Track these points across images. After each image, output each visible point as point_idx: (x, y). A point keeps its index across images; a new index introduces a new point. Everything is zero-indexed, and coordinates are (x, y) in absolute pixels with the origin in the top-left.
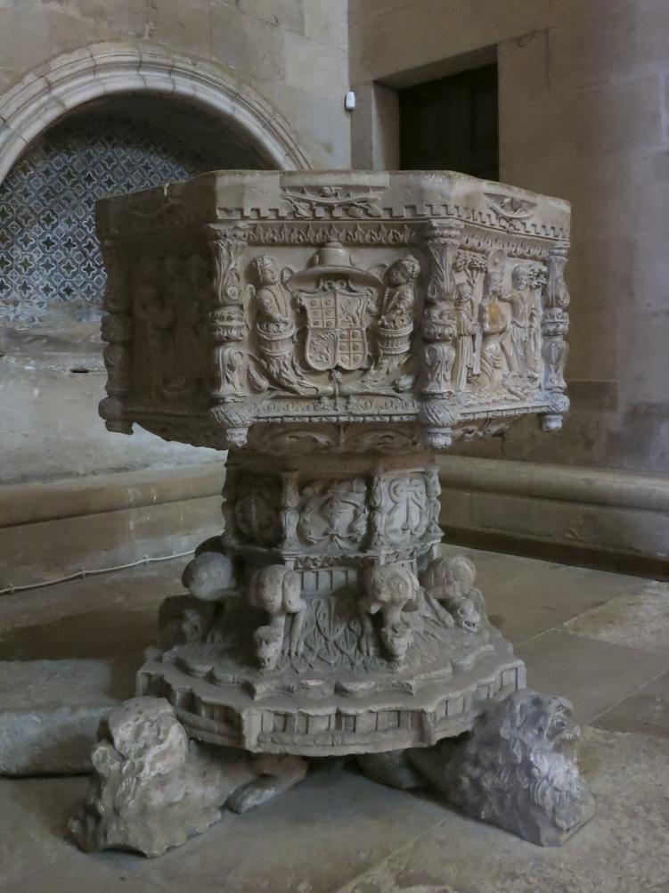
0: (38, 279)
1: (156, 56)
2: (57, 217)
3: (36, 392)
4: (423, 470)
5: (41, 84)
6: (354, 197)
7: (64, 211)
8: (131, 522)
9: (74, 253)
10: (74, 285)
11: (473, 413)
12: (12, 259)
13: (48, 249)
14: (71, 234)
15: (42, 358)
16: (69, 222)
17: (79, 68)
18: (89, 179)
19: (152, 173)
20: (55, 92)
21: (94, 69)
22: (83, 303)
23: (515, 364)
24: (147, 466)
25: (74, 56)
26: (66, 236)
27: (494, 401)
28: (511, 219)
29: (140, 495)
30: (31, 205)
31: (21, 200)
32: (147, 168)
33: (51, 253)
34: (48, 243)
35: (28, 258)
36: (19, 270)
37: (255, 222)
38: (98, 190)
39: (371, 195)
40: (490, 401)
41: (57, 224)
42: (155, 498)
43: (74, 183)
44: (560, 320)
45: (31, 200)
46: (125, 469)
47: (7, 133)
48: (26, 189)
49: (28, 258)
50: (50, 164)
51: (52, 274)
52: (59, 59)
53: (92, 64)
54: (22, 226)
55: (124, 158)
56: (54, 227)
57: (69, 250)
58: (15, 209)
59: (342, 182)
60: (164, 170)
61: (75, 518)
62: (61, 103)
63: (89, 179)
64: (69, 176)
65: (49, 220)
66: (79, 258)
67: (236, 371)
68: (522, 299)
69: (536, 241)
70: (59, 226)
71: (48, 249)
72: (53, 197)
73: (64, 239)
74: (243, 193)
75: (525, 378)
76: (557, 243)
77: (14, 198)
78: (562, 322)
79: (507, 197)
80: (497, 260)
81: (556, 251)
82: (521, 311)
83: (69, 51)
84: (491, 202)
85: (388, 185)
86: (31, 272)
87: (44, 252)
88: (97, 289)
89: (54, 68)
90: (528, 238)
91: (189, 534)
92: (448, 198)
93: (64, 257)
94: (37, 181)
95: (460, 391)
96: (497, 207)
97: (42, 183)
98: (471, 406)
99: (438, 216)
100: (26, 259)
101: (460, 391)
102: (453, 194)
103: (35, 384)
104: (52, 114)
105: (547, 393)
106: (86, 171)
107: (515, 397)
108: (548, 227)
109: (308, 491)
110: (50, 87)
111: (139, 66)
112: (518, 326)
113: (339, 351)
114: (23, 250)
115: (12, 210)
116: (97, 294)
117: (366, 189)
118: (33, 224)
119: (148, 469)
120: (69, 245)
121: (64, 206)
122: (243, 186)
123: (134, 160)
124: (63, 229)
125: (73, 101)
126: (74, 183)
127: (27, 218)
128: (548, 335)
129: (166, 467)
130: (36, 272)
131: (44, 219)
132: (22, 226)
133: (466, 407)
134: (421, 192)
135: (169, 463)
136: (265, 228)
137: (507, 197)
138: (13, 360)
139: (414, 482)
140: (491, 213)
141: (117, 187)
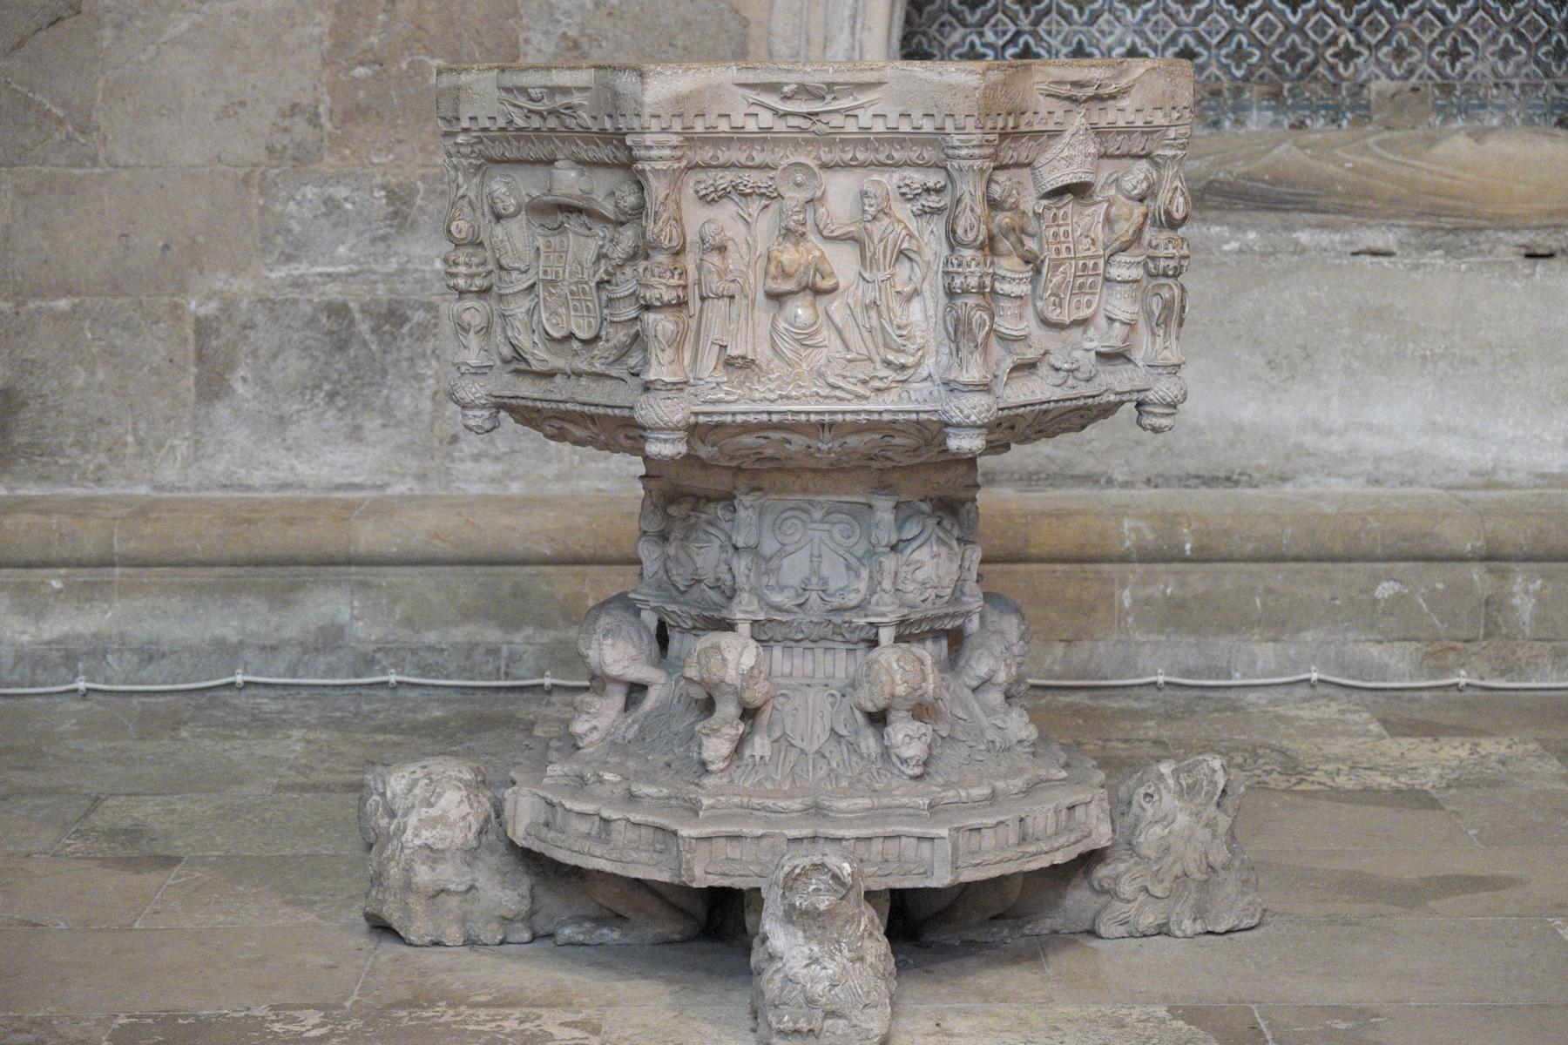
0: (1111, 33)
4: (862, 500)
6: (560, 100)
8: (1127, 592)
10: (1201, 40)
11: (734, 414)
22: (1226, 83)
23: (853, 337)
24: (1284, 479)
27: (788, 397)
28: (816, 114)
29: (1150, 536)
37: (479, 134)
39: (576, 99)
40: (773, 396)
42: (1188, 547)
44: (955, 269)
46: (1230, 481)
51: (1145, 19)
59: (543, 82)
61: (999, 567)
67: (472, 333)
68: (869, 234)
69: (894, 138)
74: (458, 98)
75: (879, 365)
76: (948, 138)
78: (958, 273)
79: (787, 84)
80: (799, 179)
81: (950, 152)
82: (868, 255)
84: (752, 95)
85: (593, 85)
86: (1094, 17)
88: (1261, 46)
90: (872, 137)
91: (1276, 640)
92: (642, 104)
95: (701, 379)
96: (774, 101)
98: (720, 401)
99: (632, 131)
101: (701, 379)
102: (648, 98)
105: (942, 389)
107: (838, 393)
108: (917, 115)
109: (673, 510)
112: (864, 279)
113: (572, 313)
116: (1262, 59)
117: (565, 91)
119: (1289, 488)
122: (458, 88)
128: (951, 293)
129: (1339, 486)
130: (1106, 16)
133: (713, 402)
134: (616, 95)
135: (1348, 477)
136: (493, 140)
137: (787, 84)
139: (833, 517)
140: (754, 109)
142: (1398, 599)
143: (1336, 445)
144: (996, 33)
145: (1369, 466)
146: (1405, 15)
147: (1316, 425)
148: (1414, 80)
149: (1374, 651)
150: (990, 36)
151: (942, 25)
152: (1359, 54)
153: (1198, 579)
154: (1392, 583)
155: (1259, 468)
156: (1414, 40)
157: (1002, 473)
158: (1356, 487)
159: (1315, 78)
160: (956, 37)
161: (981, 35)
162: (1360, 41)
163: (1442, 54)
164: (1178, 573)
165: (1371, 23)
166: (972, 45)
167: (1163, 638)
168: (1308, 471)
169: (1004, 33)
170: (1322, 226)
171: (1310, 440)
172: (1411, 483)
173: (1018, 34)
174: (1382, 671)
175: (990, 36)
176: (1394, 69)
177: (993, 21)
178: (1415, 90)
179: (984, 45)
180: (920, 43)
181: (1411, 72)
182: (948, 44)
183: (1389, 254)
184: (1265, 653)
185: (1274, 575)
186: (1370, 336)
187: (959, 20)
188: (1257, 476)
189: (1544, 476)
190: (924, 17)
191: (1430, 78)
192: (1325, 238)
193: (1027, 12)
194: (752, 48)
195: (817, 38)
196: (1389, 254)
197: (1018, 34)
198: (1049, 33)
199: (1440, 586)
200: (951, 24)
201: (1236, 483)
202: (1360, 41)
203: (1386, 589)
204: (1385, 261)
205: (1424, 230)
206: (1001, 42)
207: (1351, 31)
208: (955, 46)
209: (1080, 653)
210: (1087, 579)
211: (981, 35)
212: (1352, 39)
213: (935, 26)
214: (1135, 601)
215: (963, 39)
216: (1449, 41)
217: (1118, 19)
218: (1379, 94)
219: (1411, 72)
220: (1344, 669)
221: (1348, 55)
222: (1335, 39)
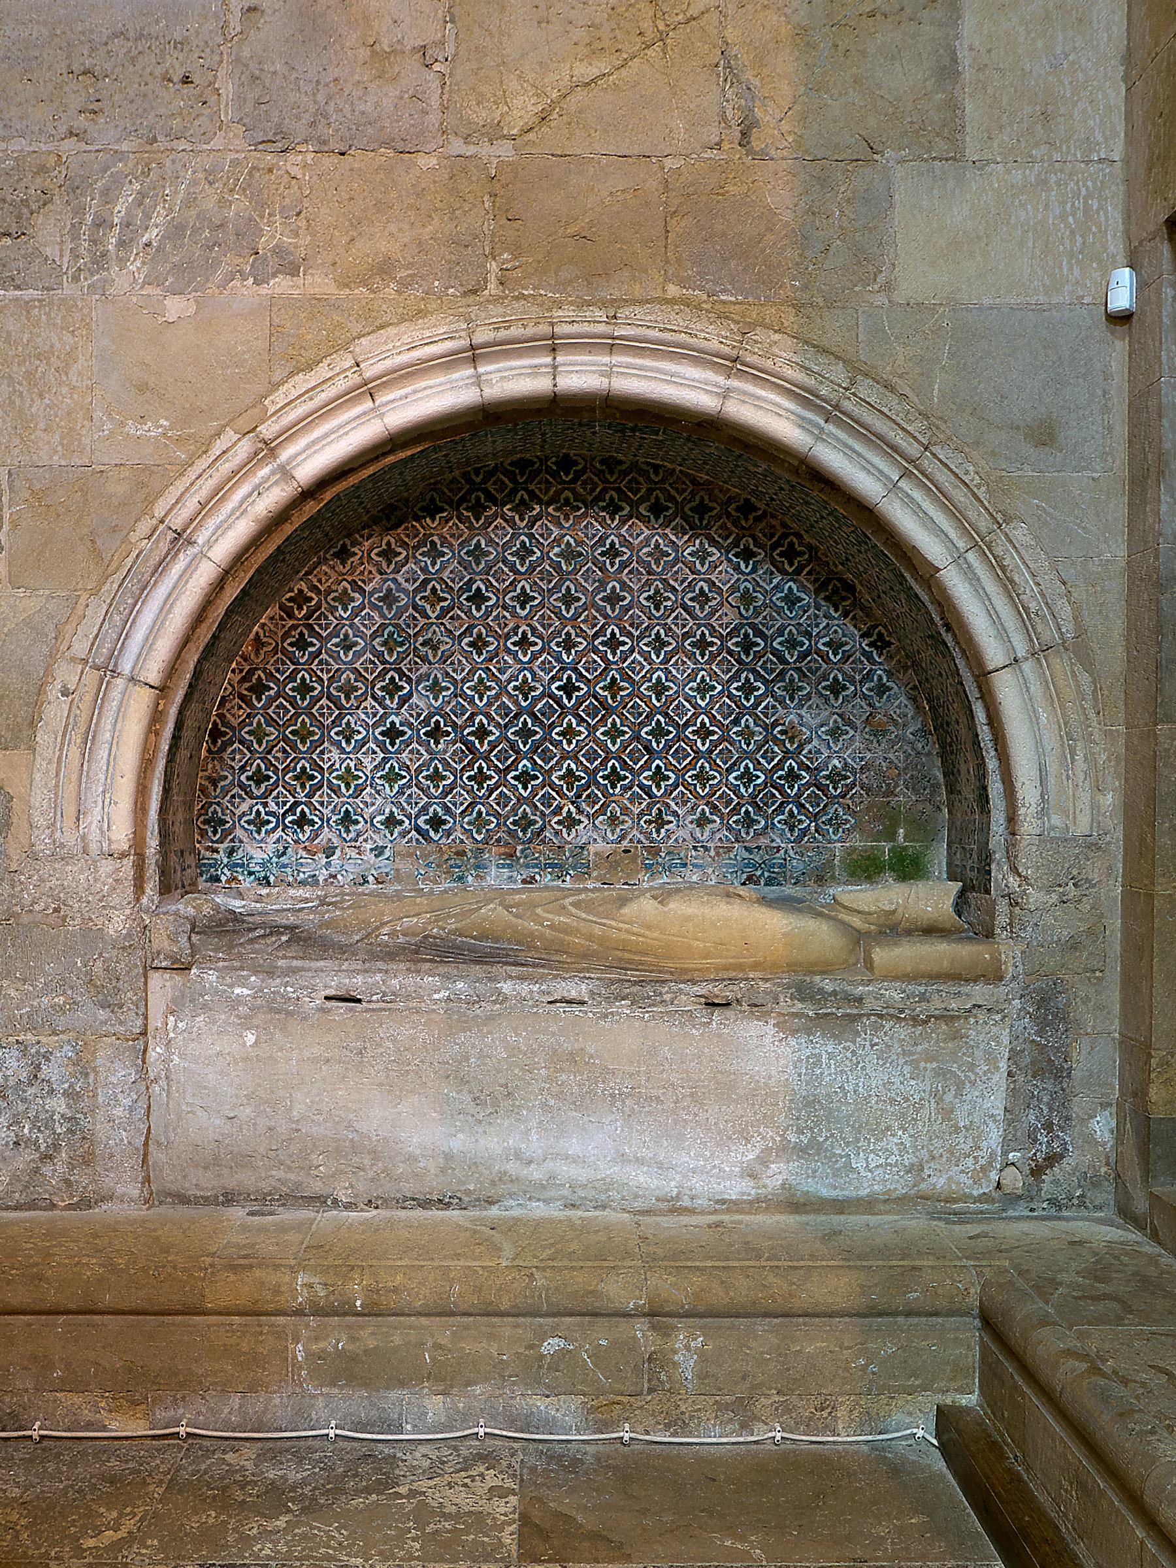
0: (373, 804)
1: (508, 325)
2: (409, 681)
3: (250, 1038)
5: (244, 449)
7: (424, 669)
9: (447, 747)
10: (447, 810)
12: (321, 770)
13: (393, 744)
14: (439, 711)
15: (271, 973)
16: (436, 688)
17: (324, 396)
18: (478, 598)
19: (624, 565)
20: (284, 455)
21: (368, 389)
22: (469, 845)
24: (491, 1202)
25: (322, 371)
26: (430, 716)
30: (357, 665)
31: (337, 659)
32: (612, 552)
33: (399, 752)
34: (392, 733)
35: (352, 765)
36: (336, 791)
38: (497, 617)
41: (410, 694)
42: (358, 1303)
43: (445, 612)
45: (358, 655)
47: (192, 551)
48: (346, 635)
49: (352, 765)
50: (395, 580)
51: (401, 792)
52: (283, 389)
53: (357, 379)
54: (340, 707)
55: (558, 541)
56: (403, 701)
57: (437, 743)
58: (325, 677)
60: (658, 553)
62: (285, 473)
63: (478, 598)
64: (435, 598)
65: (392, 689)
66: (458, 756)
70: (415, 699)
71: (393, 744)
72: (402, 644)
73: (426, 722)
77: (324, 656)
83: (309, 367)
86: (359, 790)
87: (384, 750)
88: (497, 815)
89: (271, 410)
91: (444, 1393)
93: (426, 756)
94: (371, 618)
97: (380, 621)
100: (348, 769)
103: (246, 1023)
104: (275, 497)
106: (471, 582)
110: (268, 449)
111: (474, 354)
114: (343, 751)
115: (321, 680)
116: (498, 825)
118: (362, 699)
119: (494, 1211)
120: (436, 733)
121: (425, 659)
123: (580, 543)
124: (422, 704)
125: (309, 469)
126: (445, 612)
127: (348, 690)
129: (538, 1210)
131: (382, 689)
132: (340, 707)
135: (547, 1201)
138: (212, 977)
141: (542, 605)
142: (562, 1353)
143: (536, 1173)
144: (277, 804)
145: (566, 1192)
146: (617, 790)
147: (518, 1155)
148: (625, 843)
149: (541, 1404)
150: (273, 807)
151: (233, 797)
152: (580, 822)
153: (369, 1336)
154: (557, 1340)
155: (468, 1192)
156: (625, 811)
157: (240, 1194)
158: (554, 1211)
159: (543, 841)
160: (244, 807)
161: (265, 805)
162: (580, 811)
163: (649, 822)
164: (350, 1327)
165: (588, 796)
166: (258, 812)
167: (335, 1391)
168: (511, 1195)
169: (285, 803)
170: (522, 978)
171: (513, 1167)
172: (604, 1207)
173: (296, 804)
174: (550, 1425)
175: (273, 807)
176: (609, 834)
177: (275, 793)
178: (626, 851)
179: (266, 814)
180: (215, 812)
181: (623, 837)
182: (238, 812)
183: (583, 1003)
184: (435, 1405)
185: (442, 1332)
186: (564, 1077)
187: (246, 793)
188: (466, 1199)
189: (723, 1202)
190: (218, 790)
191: (639, 842)
192: (525, 988)
193: (303, 786)
194: (15, 820)
195: (70, 811)
196: (583, 1003)
197: (296, 804)
198: (322, 804)
199: (603, 1343)
200: (240, 796)
201: (448, 1205)
202: (580, 811)
203: (552, 1345)
204: (576, 1008)
205: (612, 982)
206: (281, 811)
207: (573, 803)
208: (244, 814)
209: (257, 1404)
210: (261, 1333)
211: (265, 805)
212: (573, 810)
213: (228, 798)
214: (309, 1355)
215: (251, 808)
216: (654, 811)
217: (378, 792)
218: (596, 854)
219: (623, 837)
220: (511, 1423)
221: (570, 822)
222: (560, 808)
